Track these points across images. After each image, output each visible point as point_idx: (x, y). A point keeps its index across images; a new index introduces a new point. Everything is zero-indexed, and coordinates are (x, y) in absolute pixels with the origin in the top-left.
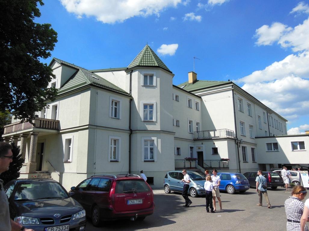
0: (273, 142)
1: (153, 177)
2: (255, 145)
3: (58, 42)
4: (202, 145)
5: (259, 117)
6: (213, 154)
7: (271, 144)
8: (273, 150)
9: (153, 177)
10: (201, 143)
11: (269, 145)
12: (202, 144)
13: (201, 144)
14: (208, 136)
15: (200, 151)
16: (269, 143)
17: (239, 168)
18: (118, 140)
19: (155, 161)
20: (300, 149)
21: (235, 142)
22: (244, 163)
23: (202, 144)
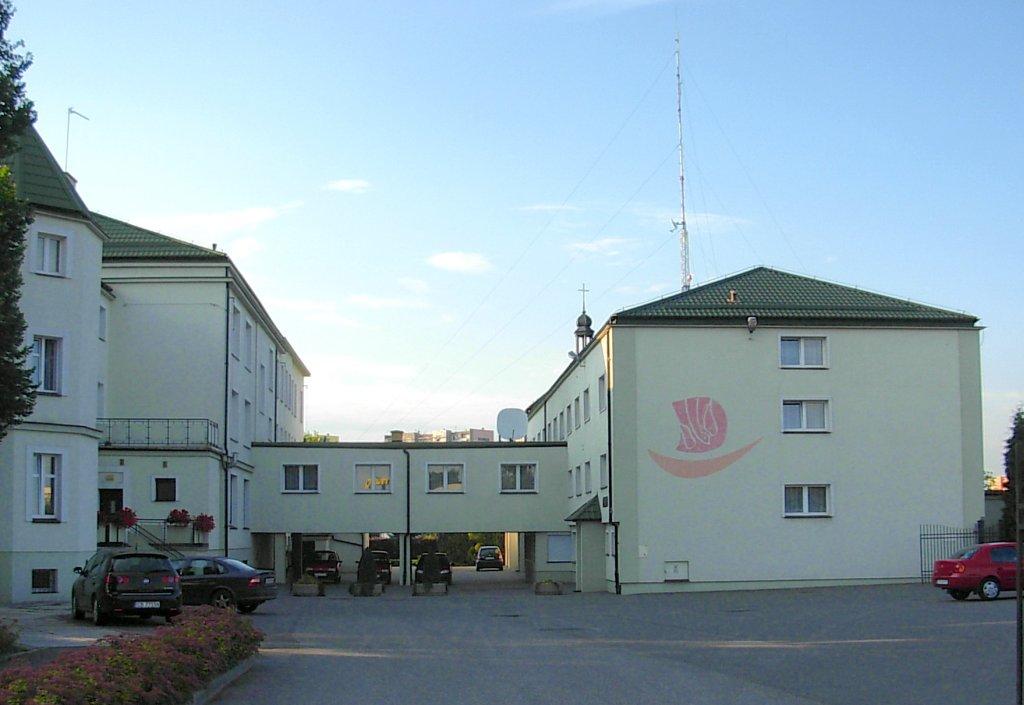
0: (304, 464)
1: (34, 572)
2: (249, 469)
3: (35, 103)
4: (121, 469)
5: (262, 367)
6: (157, 500)
7: (297, 467)
8: (301, 490)
9: (34, 572)
10: (162, 459)
11: (290, 470)
12: (122, 462)
13: (119, 462)
14: (203, 440)
15: (111, 486)
16: (291, 466)
17: (224, 547)
18: (59, 456)
19: (63, 520)
20: (809, 511)
21: (222, 460)
22: (35, 525)
23: (122, 462)
